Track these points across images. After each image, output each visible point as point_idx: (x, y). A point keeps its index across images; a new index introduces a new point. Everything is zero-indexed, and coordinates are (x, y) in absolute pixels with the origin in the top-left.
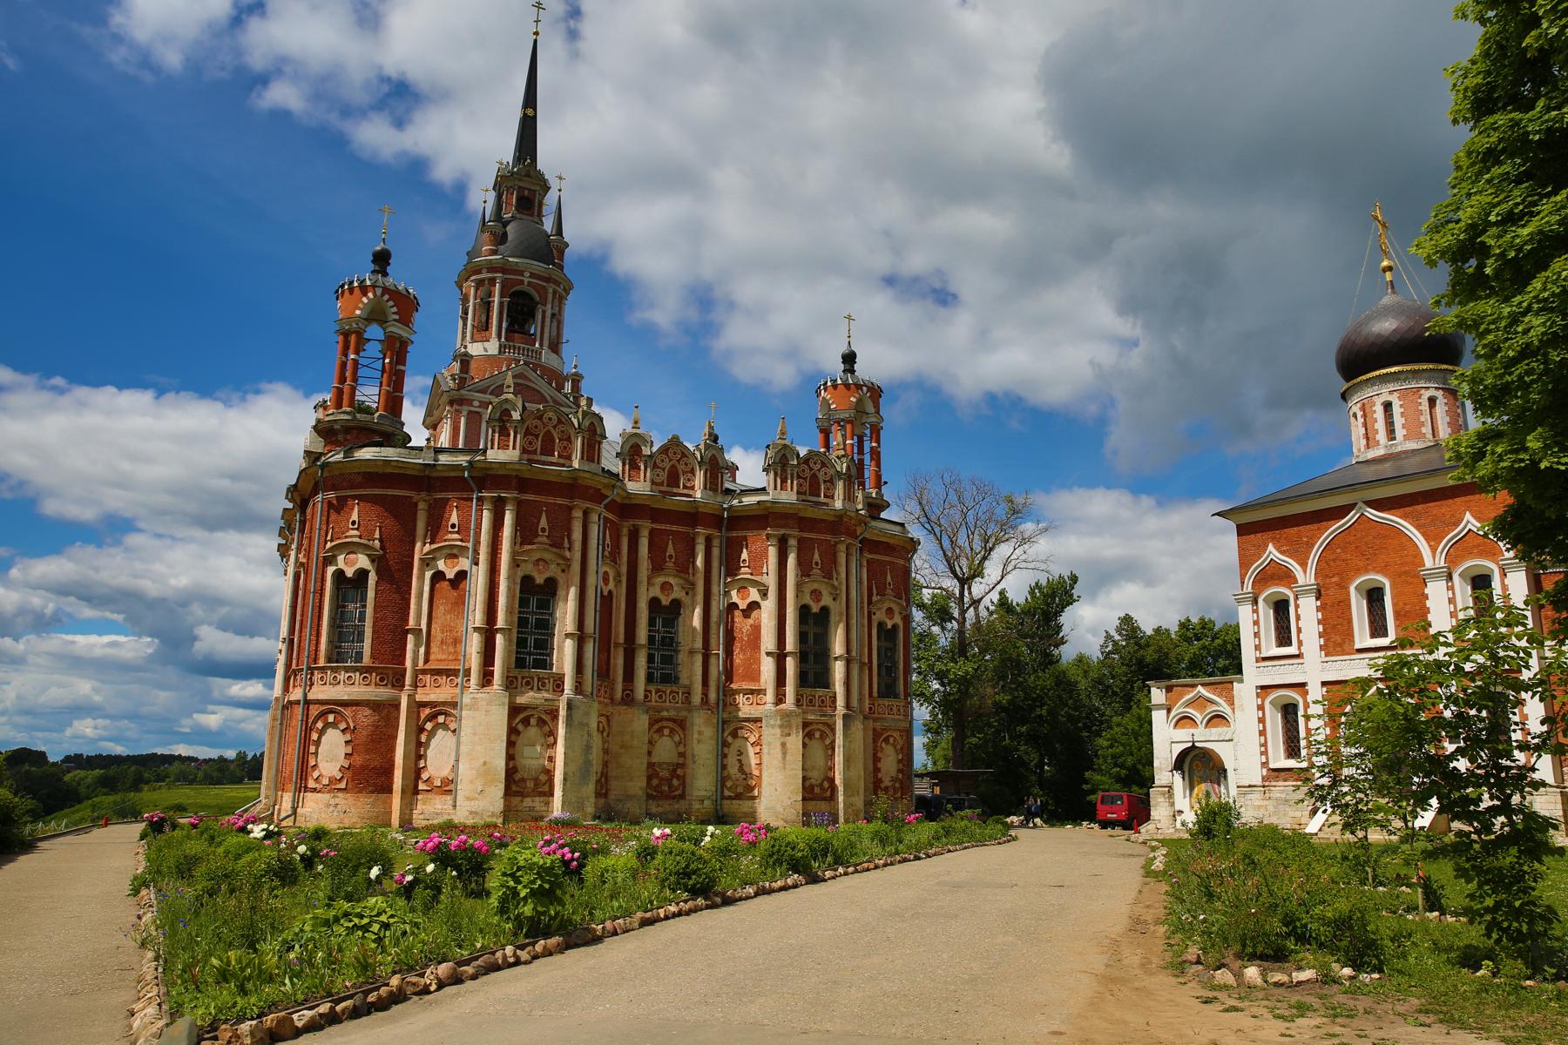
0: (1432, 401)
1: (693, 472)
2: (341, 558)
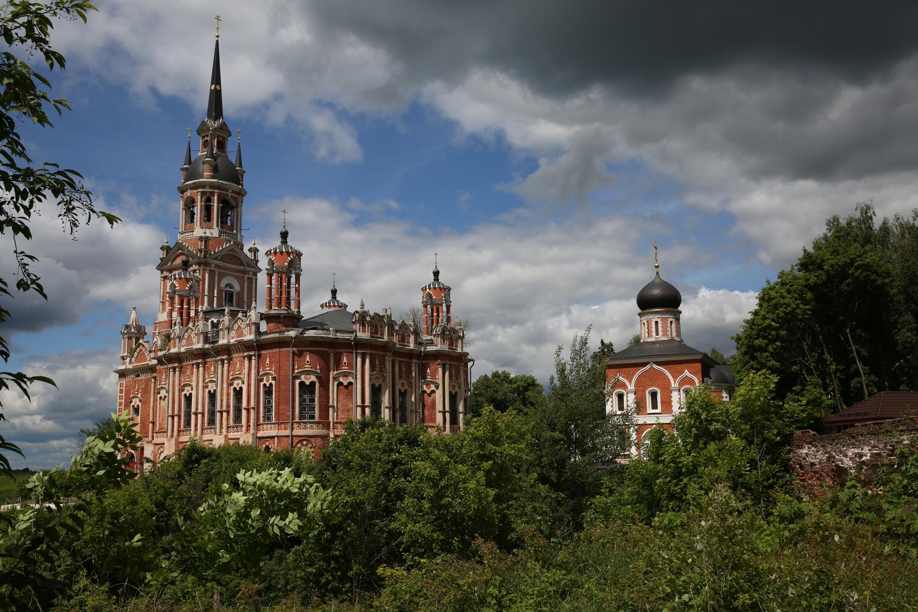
0: (671, 322)
1: (409, 336)
2: (303, 377)
